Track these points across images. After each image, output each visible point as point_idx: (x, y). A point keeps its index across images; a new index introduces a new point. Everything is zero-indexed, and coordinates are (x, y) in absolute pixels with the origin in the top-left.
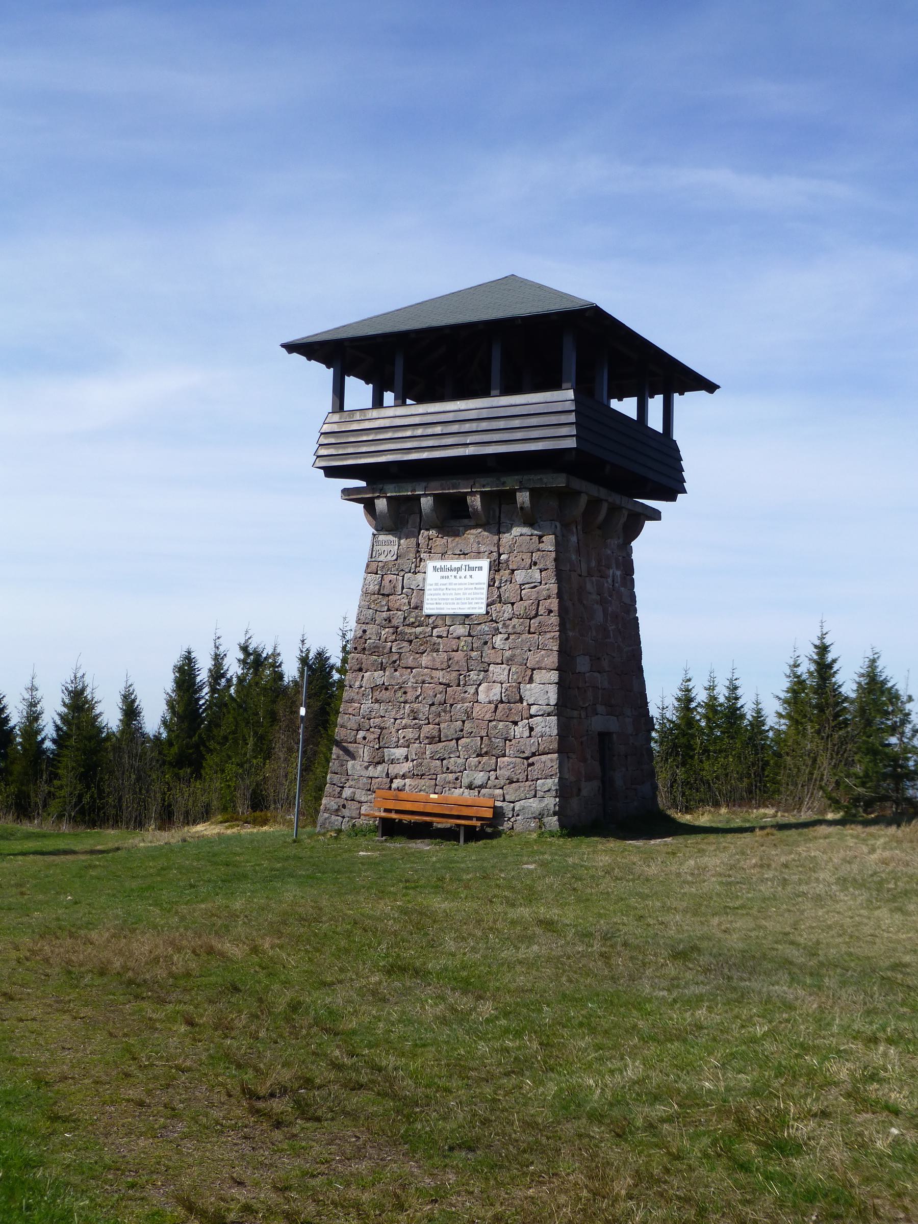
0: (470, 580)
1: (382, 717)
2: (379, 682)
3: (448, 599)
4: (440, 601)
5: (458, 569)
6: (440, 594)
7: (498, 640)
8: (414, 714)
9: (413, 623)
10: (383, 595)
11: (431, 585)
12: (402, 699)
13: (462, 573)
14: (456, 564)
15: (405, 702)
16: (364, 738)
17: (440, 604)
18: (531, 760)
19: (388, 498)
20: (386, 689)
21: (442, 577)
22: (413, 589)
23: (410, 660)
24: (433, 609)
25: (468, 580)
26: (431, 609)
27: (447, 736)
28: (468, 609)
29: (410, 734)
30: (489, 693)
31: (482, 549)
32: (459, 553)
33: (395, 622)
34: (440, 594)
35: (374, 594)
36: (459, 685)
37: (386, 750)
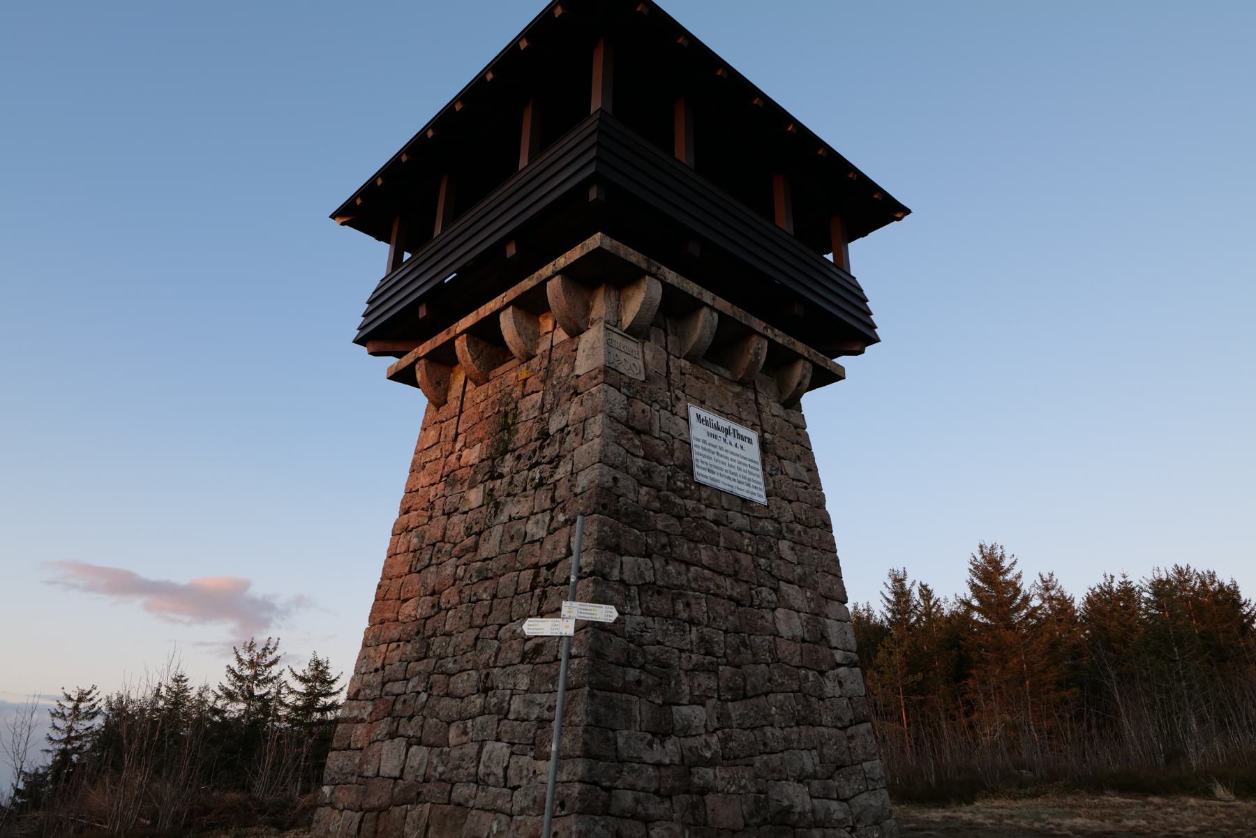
0: (738, 451)
1: (659, 643)
2: (649, 576)
3: (722, 469)
4: (715, 470)
5: (727, 432)
6: (710, 458)
7: (784, 546)
8: (706, 645)
9: (681, 490)
10: (632, 428)
11: (698, 440)
12: (685, 615)
13: (729, 438)
14: (724, 423)
15: (691, 622)
16: (639, 682)
17: (714, 473)
18: (850, 731)
19: (667, 287)
20: (659, 593)
21: (709, 434)
22: (673, 438)
23: (684, 549)
24: (707, 477)
25: (738, 451)
26: (703, 476)
27: (754, 688)
28: (748, 492)
29: (705, 681)
30: (790, 624)
31: (744, 415)
32: (717, 408)
33: (658, 480)
34: (710, 458)
35: (619, 422)
36: (751, 606)
37: (674, 708)
